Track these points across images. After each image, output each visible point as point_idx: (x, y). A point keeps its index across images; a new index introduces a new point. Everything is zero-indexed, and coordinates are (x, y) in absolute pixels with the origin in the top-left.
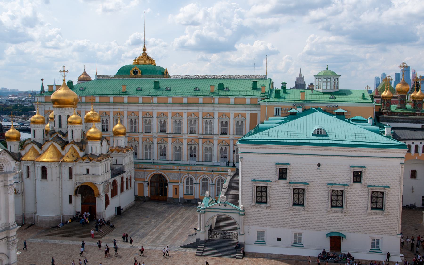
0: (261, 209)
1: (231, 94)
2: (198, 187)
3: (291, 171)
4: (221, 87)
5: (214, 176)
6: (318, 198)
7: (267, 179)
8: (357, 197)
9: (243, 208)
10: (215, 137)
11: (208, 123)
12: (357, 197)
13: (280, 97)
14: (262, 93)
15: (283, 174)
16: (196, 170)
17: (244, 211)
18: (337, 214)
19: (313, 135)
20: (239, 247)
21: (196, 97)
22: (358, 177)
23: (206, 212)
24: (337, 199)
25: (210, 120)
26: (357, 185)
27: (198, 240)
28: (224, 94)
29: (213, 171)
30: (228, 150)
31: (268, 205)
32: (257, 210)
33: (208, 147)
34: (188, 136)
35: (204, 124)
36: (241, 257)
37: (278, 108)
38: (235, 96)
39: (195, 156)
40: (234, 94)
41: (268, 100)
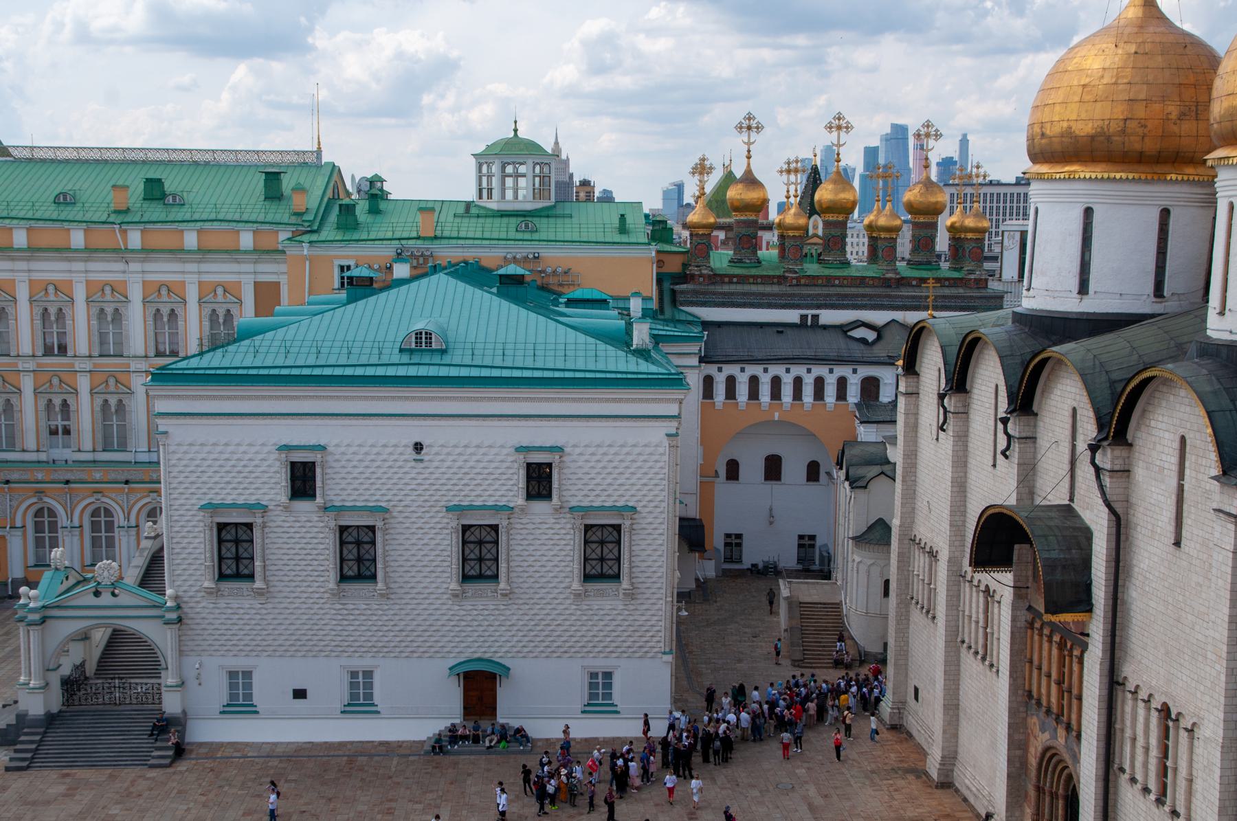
0: (239, 599)
1: (188, 217)
2: (76, 539)
3: (329, 471)
4: (155, 190)
5: (133, 499)
6: (421, 553)
8: (543, 546)
9: (176, 598)
10: (134, 365)
11: (109, 318)
12: (543, 546)
13: (356, 226)
14: (295, 214)
15: (303, 480)
16: (67, 482)
17: (179, 607)
18: (482, 599)
19: (401, 350)
20: (164, 726)
21: (58, 225)
22: (539, 481)
23: (49, 622)
24: (480, 552)
25: (113, 306)
26: (539, 506)
27: (21, 717)
28: (163, 217)
29: (127, 482)
30: (72, 408)
31: (259, 584)
32: (222, 603)
33: (113, 401)
34: (39, 365)
35: (94, 322)
36: (167, 761)
37: (345, 263)
38: (199, 224)
39: (67, 431)
40: (196, 217)
41: (314, 237)
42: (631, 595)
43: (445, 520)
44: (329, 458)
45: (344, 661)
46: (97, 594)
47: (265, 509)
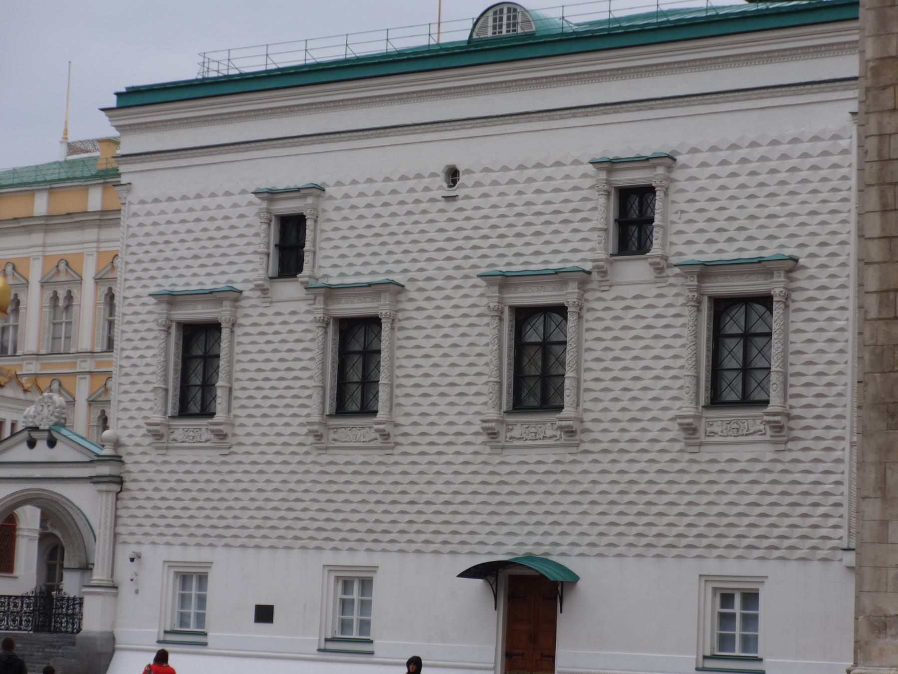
3: (326, 226)
7: (221, 283)
8: (637, 345)
15: (290, 244)
22: (633, 217)
26: (634, 269)
42: (781, 430)
43: (485, 301)
44: (328, 205)
45: (329, 558)
46: (32, 444)
47: (234, 295)
